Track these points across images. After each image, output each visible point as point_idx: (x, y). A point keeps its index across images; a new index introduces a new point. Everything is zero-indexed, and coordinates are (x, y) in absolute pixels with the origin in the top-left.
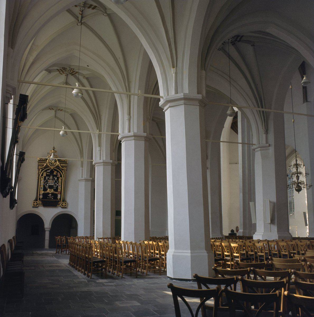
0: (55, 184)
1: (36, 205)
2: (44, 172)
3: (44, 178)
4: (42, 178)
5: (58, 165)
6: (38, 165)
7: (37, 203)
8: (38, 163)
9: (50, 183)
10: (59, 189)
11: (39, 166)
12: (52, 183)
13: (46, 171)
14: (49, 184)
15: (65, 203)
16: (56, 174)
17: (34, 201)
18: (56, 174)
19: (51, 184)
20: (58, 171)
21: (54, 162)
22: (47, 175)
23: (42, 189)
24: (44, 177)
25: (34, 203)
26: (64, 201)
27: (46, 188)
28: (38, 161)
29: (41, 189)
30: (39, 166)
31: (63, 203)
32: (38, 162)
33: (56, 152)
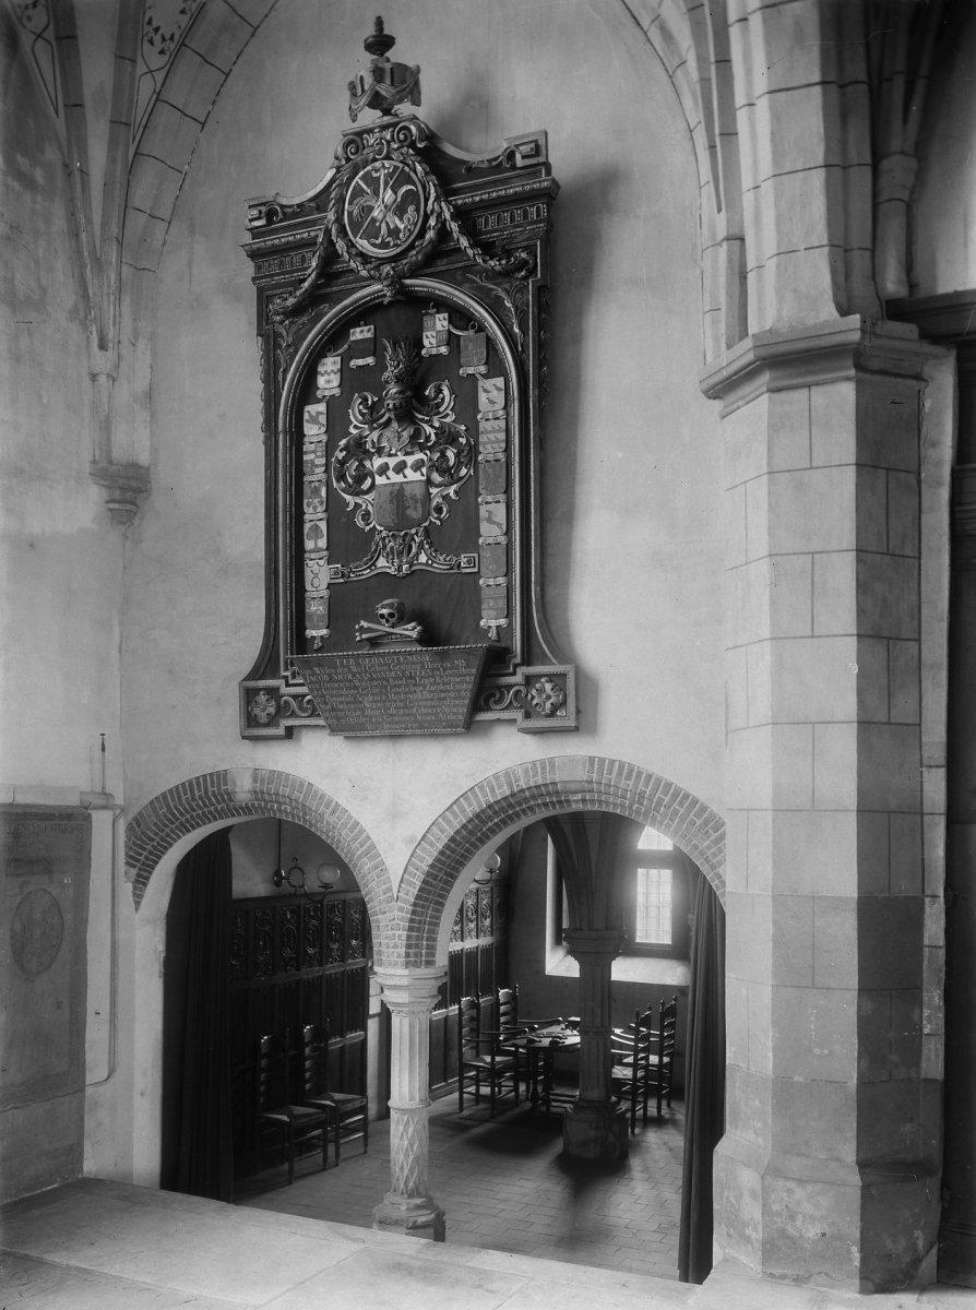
0: (443, 469)
1: (272, 721)
2: (317, 355)
3: (323, 419)
4: (314, 420)
5: (443, 233)
6: (260, 291)
7: (273, 693)
8: (249, 268)
9: (392, 462)
10: (490, 520)
11: (269, 299)
12: (410, 460)
13: (333, 339)
14: (383, 470)
15: (558, 680)
16: (444, 350)
17: (247, 678)
18: (444, 350)
19: (400, 468)
20: (460, 317)
21: (400, 211)
22: (352, 381)
23: (322, 543)
24: (322, 407)
25: (249, 695)
26: (544, 660)
27: (360, 523)
28: (247, 238)
29: (309, 545)
30: (264, 299)
31: (529, 680)
32: (254, 255)
33: (406, 82)
